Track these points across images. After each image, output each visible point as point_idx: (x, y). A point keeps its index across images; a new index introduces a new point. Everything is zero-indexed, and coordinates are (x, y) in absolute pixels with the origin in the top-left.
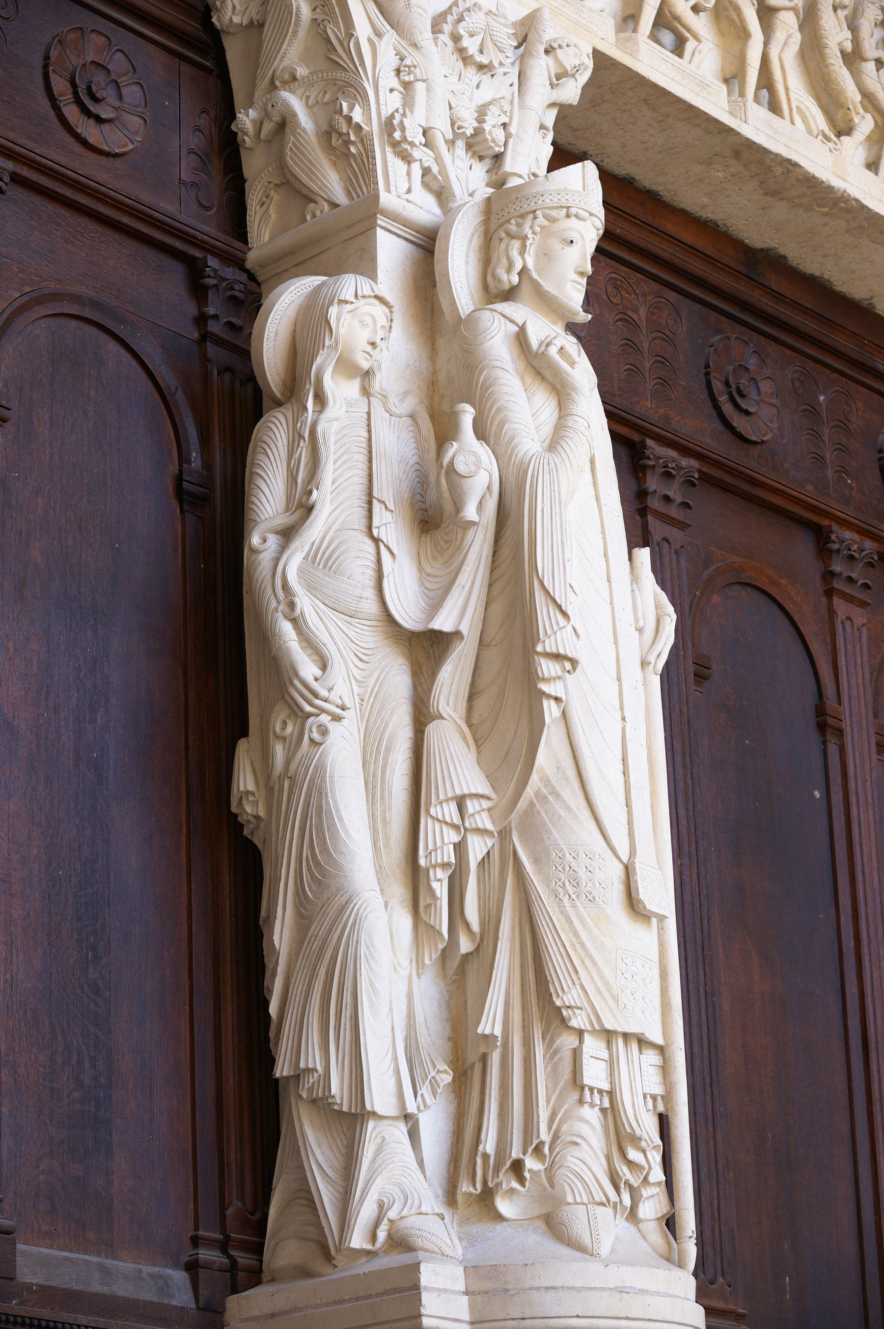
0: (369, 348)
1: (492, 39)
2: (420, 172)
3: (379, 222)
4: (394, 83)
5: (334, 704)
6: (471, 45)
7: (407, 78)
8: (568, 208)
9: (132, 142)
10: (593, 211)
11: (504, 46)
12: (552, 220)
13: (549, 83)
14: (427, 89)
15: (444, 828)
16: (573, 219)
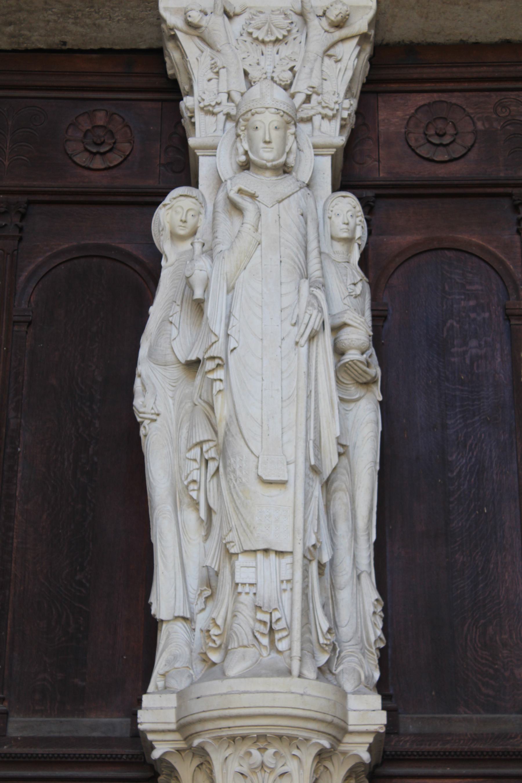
0: (181, 224)
1: (274, 26)
2: (224, 117)
3: (198, 154)
4: (212, 75)
5: (149, 413)
6: (261, 35)
7: (215, 71)
8: (251, 110)
9: (121, 157)
10: (267, 106)
11: (281, 26)
12: (247, 120)
13: (323, 31)
14: (227, 71)
15: (192, 462)
16: (256, 115)
